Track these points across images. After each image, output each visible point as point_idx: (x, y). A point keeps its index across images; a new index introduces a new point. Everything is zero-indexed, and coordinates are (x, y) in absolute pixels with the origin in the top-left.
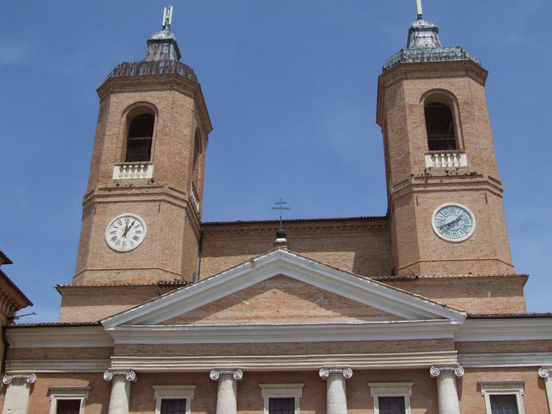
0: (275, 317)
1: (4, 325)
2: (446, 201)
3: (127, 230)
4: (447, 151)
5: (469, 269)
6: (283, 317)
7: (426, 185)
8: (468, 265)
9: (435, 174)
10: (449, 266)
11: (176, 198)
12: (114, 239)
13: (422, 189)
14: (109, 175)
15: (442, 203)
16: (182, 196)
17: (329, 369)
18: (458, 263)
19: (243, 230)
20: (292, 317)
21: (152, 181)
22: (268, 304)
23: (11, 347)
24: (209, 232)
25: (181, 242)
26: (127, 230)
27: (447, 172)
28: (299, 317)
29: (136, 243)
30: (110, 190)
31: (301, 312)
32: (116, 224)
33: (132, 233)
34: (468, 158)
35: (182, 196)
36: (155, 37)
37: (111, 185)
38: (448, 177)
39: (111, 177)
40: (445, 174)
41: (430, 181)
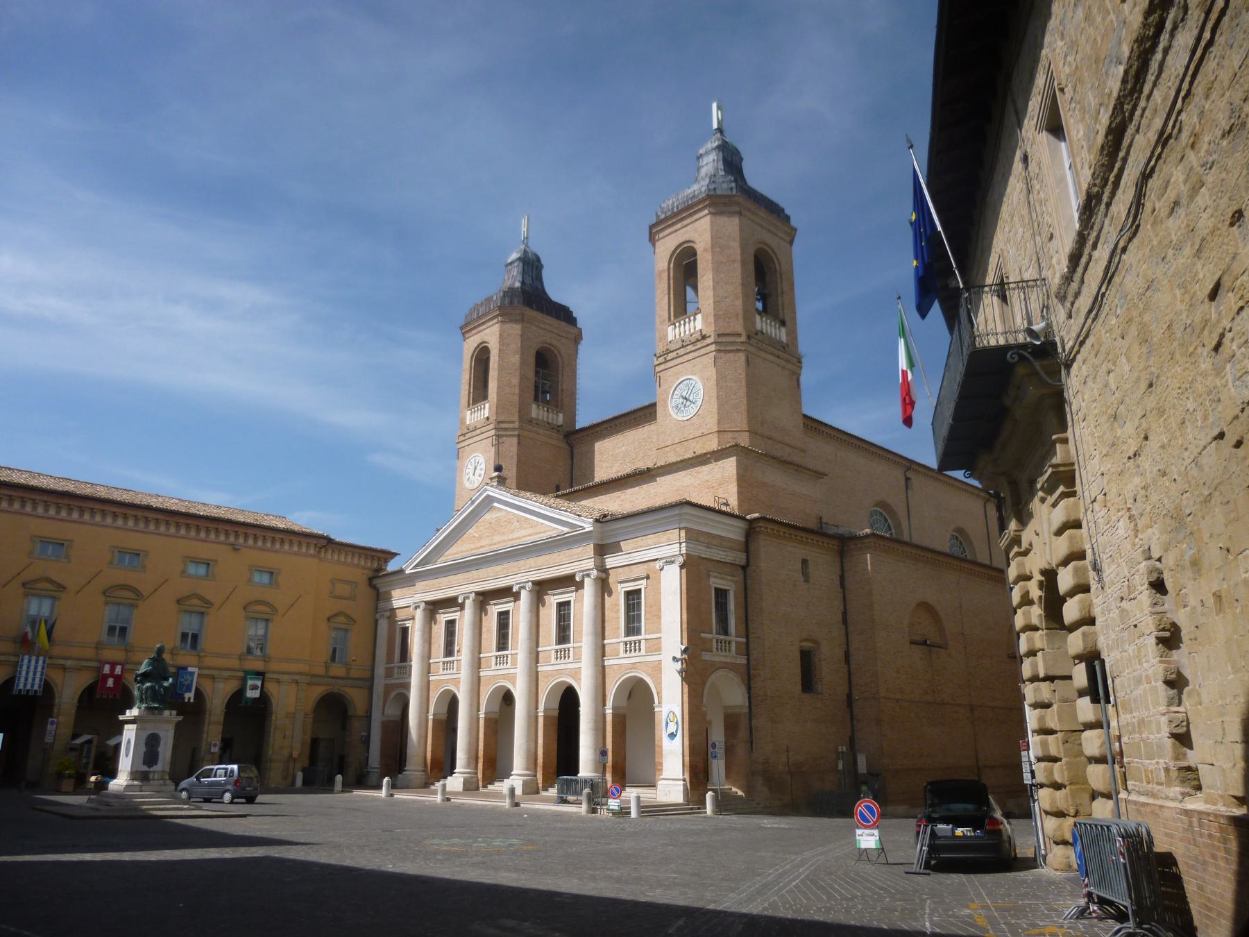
0: (491, 545)
1: (370, 576)
2: (682, 376)
3: (475, 468)
5: (694, 447)
6: (495, 544)
7: (666, 361)
8: (693, 443)
9: (673, 347)
10: (679, 449)
11: (506, 429)
12: (468, 479)
13: (662, 367)
14: (463, 421)
15: (678, 379)
16: (511, 426)
17: (519, 584)
18: (686, 443)
19: (597, 432)
20: (499, 542)
21: (488, 418)
22: (486, 534)
23: (381, 591)
24: (574, 440)
25: (515, 469)
26: (475, 468)
27: (683, 341)
28: (504, 541)
29: (480, 479)
30: (463, 435)
31: (505, 538)
33: (478, 471)
35: (511, 426)
36: (509, 261)
37: (466, 431)
38: (683, 346)
39: (465, 423)
40: (680, 345)
41: (671, 356)
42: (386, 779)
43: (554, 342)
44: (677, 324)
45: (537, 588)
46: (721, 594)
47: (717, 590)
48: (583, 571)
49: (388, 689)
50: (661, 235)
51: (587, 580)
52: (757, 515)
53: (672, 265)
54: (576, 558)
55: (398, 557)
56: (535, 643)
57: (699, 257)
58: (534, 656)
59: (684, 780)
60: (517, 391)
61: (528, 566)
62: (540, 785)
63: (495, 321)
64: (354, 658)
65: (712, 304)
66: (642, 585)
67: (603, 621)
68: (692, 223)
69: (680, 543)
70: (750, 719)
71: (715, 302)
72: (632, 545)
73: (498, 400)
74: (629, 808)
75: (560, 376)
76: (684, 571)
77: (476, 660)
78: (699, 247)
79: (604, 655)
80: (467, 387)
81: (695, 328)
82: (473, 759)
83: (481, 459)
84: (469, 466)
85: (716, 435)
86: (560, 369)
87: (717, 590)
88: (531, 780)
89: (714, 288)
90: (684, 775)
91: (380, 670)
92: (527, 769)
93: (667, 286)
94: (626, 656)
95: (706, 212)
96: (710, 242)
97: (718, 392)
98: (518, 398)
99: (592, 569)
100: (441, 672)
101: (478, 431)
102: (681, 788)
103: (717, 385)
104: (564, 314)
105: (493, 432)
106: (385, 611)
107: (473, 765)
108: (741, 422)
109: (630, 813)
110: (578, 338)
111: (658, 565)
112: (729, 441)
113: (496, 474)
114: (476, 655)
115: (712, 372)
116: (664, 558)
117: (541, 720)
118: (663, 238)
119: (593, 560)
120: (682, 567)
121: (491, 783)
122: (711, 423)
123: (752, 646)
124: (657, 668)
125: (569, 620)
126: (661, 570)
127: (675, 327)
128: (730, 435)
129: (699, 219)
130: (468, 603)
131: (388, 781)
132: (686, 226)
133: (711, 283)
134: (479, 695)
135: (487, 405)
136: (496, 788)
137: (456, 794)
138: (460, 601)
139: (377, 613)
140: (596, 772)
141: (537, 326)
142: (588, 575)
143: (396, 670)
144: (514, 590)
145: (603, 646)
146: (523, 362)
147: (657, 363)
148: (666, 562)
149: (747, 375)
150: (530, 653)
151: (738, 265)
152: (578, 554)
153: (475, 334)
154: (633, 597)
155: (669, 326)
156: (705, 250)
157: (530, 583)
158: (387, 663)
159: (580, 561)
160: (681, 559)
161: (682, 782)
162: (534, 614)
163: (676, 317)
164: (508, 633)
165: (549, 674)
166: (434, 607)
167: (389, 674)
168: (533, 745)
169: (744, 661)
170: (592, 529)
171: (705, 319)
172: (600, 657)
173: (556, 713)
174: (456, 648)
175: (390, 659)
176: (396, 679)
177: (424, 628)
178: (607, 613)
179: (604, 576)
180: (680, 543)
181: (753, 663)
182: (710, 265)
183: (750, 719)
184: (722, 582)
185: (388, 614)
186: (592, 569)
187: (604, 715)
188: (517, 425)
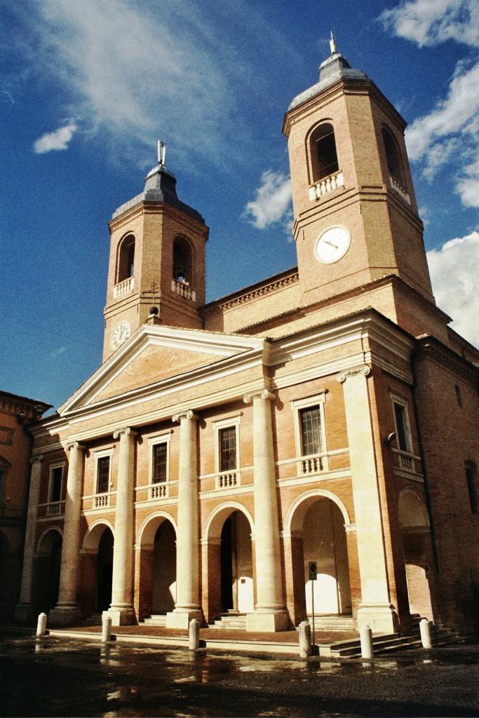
4: (325, 178)
12: (115, 343)
16: (156, 295)
24: (206, 313)
32: (116, 332)
34: (344, 176)
42: (41, 616)
43: (188, 235)
44: (318, 186)
45: (198, 417)
46: (399, 409)
47: (395, 404)
48: (252, 392)
49: (40, 527)
50: (296, 120)
51: (256, 401)
52: (425, 335)
53: (308, 141)
54: (242, 381)
55: (51, 408)
56: (195, 472)
57: (335, 131)
58: (195, 484)
59: (392, 607)
60: (159, 268)
61: (188, 395)
62: (207, 618)
63: (141, 213)
64: (8, 498)
65: (353, 165)
66: (319, 400)
67: (275, 443)
68: (327, 104)
69: (365, 353)
70: (433, 539)
71: (356, 162)
72: (305, 362)
73: (143, 275)
74: (358, 643)
75: (193, 261)
76: (371, 380)
77: (132, 493)
78: (335, 124)
79: (277, 476)
80: (114, 269)
81: (336, 186)
82: (130, 593)
83: (127, 325)
84: (116, 332)
85: (368, 271)
86: (193, 257)
87: (395, 404)
88: (197, 613)
89: (354, 151)
90: (390, 601)
91: (33, 510)
92: (193, 602)
93: (305, 157)
94: (305, 475)
95: (341, 93)
96: (346, 116)
97: (366, 235)
98: (160, 274)
99: (262, 390)
100: (94, 507)
101: (124, 302)
102: (390, 617)
103: (365, 229)
104: (194, 217)
105: (139, 301)
106: (39, 455)
107: (129, 600)
108: (390, 259)
109: (359, 650)
110: (206, 235)
111: (339, 378)
112: (381, 275)
113: (153, 315)
114: (132, 488)
115: (359, 219)
116: (346, 370)
117: (205, 550)
118: (299, 121)
119: (263, 380)
120: (367, 377)
121: (148, 617)
122: (362, 261)
123: (428, 464)
124: (345, 487)
125: (234, 445)
126: (342, 383)
127: (316, 187)
128: (381, 270)
129: (333, 100)
130: (124, 438)
131: (44, 618)
132: (321, 108)
133: (350, 147)
134: (134, 529)
135: (133, 281)
136: (155, 622)
137: (115, 629)
138: (115, 437)
139: (31, 457)
140: (277, 603)
141: (174, 219)
142: (259, 396)
143: (48, 508)
144: (173, 420)
145: (277, 468)
146: (164, 245)
147: (301, 219)
148: (349, 374)
149: (391, 222)
150: (192, 481)
151: (373, 135)
152: (244, 377)
153: (121, 227)
154: (308, 417)
155: (310, 188)
156: (342, 123)
157: (191, 413)
158: (40, 503)
159: (248, 382)
160: (367, 369)
161: (390, 611)
162: (195, 443)
163: (314, 181)
164: (164, 466)
165: (215, 502)
166: (86, 447)
167: (42, 513)
168: (197, 575)
169: (422, 480)
170: (262, 348)
171: (347, 178)
172: (274, 479)
173: (218, 542)
174: (110, 484)
175: (42, 498)
176: (47, 517)
177: (77, 466)
178: (278, 434)
179: (274, 396)
180: (365, 353)
181: (430, 481)
182: (349, 134)
183: (433, 539)
184: (399, 399)
185: (42, 457)
186: (262, 390)
187: (281, 540)
188: (159, 295)
